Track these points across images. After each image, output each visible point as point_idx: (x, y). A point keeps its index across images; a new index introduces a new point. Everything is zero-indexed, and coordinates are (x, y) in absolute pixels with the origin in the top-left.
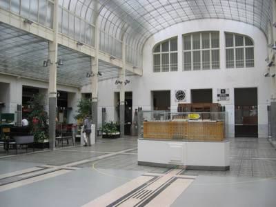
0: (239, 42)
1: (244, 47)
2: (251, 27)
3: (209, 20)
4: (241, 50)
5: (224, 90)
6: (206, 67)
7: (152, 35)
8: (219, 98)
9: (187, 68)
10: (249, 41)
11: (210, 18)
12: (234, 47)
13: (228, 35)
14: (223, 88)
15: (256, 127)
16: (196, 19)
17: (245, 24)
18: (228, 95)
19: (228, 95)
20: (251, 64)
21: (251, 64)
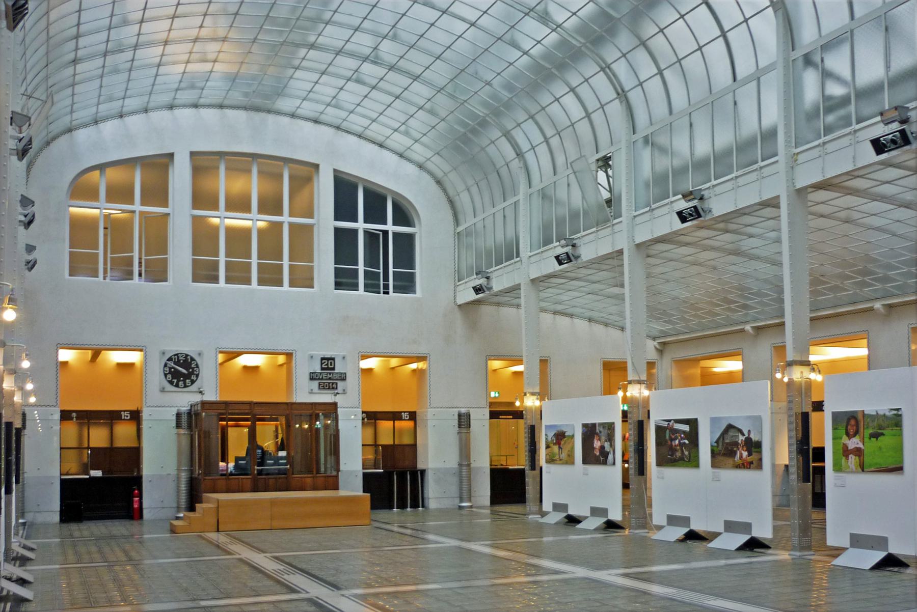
0: (375, 212)
1: (390, 227)
2: (411, 169)
3: (286, 120)
4: (374, 242)
5: (333, 359)
6: (270, 277)
7: (70, 130)
8: (316, 383)
9: (205, 273)
10: (403, 216)
11: (293, 116)
12: (361, 225)
13: (345, 188)
14: (328, 354)
15: (418, 476)
16: (245, 108)
17: (395, 158)
18: (343, 377)
19: (343, 377)
20: (406, 284)
21: (406, 284)
